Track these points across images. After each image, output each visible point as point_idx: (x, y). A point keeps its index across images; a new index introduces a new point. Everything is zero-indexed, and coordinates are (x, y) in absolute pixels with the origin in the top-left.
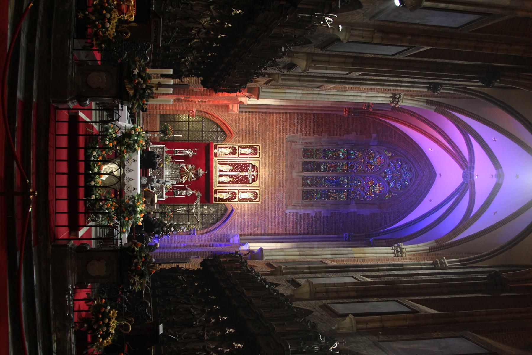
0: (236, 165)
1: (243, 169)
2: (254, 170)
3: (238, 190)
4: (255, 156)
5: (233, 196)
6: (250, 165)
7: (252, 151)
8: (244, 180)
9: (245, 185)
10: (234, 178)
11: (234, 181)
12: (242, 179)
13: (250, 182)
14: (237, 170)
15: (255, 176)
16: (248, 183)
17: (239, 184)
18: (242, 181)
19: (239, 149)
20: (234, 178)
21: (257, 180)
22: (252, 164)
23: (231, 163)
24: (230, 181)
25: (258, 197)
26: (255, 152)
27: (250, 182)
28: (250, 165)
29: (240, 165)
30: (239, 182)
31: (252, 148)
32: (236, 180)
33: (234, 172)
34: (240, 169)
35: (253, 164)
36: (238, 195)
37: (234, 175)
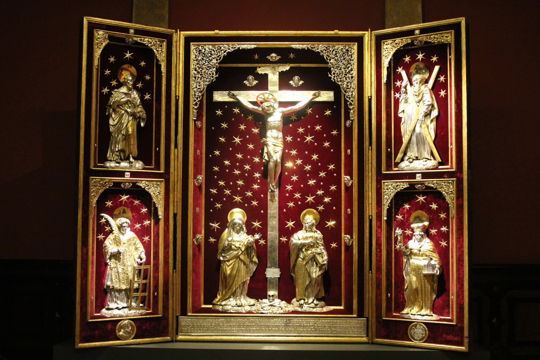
0: (221, 190)
1: (245, 142)
2: (253, 71)
3: (381, 177)
4: (161, 56)
5: (424, 207)
6: (220, 97)
7: (127, 76)
8: (318, 137)
9: (349, 131)
10: (303, 199)
11: (319, 201)
12: (312, 148)
13: (327, 96)
14: (249, 180)
15: (286, 68)
16: (336, 113)
17: (338, 169)
18: (320, 150)
19: (111, 165)
20: (303, 199)
21: (317, 57)
22: (212, 88)
23: (209, 218)
24: (320, 226)
25: (424, 38)
26: (134, 62)
27: (327, 96)
28: (220, 97)
29: (218, 161)
30: (329, 173)
31: (105, 81)
32: (311, 190)
33: (264, 205)
34: (244, 161)
35: (211, 74)
36: (413, 175)
37: (282, 205)
